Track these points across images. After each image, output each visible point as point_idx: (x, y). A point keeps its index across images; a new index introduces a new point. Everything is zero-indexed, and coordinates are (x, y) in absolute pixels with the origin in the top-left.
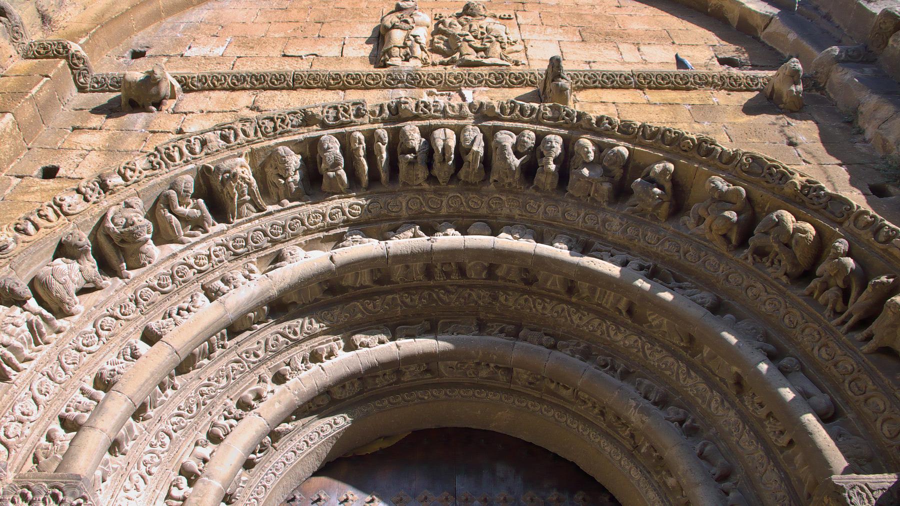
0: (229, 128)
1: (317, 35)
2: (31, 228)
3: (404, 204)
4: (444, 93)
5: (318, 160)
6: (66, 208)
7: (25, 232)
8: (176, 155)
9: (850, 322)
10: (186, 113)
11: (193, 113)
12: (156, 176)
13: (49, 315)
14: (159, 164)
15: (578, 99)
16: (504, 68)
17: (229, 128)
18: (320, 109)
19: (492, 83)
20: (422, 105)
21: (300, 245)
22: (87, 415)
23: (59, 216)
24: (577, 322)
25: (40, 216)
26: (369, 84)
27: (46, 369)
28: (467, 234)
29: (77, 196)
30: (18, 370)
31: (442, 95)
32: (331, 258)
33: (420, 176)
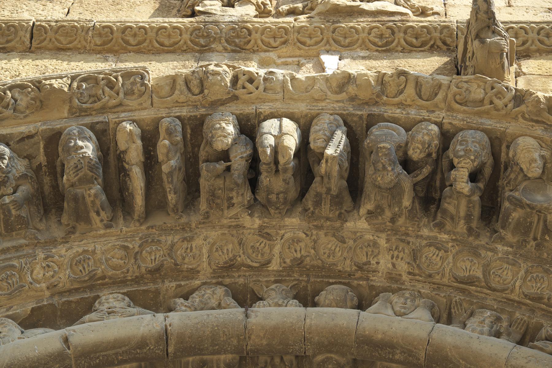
3: (205, 251)
4: (290, 60)
5: (59, 169)
15: (524, 70)
19: (375, 44)
21: (13, 318)
26: (162, 44)
28: (315, 305)
32: (66, 340)
33: (235, 201)
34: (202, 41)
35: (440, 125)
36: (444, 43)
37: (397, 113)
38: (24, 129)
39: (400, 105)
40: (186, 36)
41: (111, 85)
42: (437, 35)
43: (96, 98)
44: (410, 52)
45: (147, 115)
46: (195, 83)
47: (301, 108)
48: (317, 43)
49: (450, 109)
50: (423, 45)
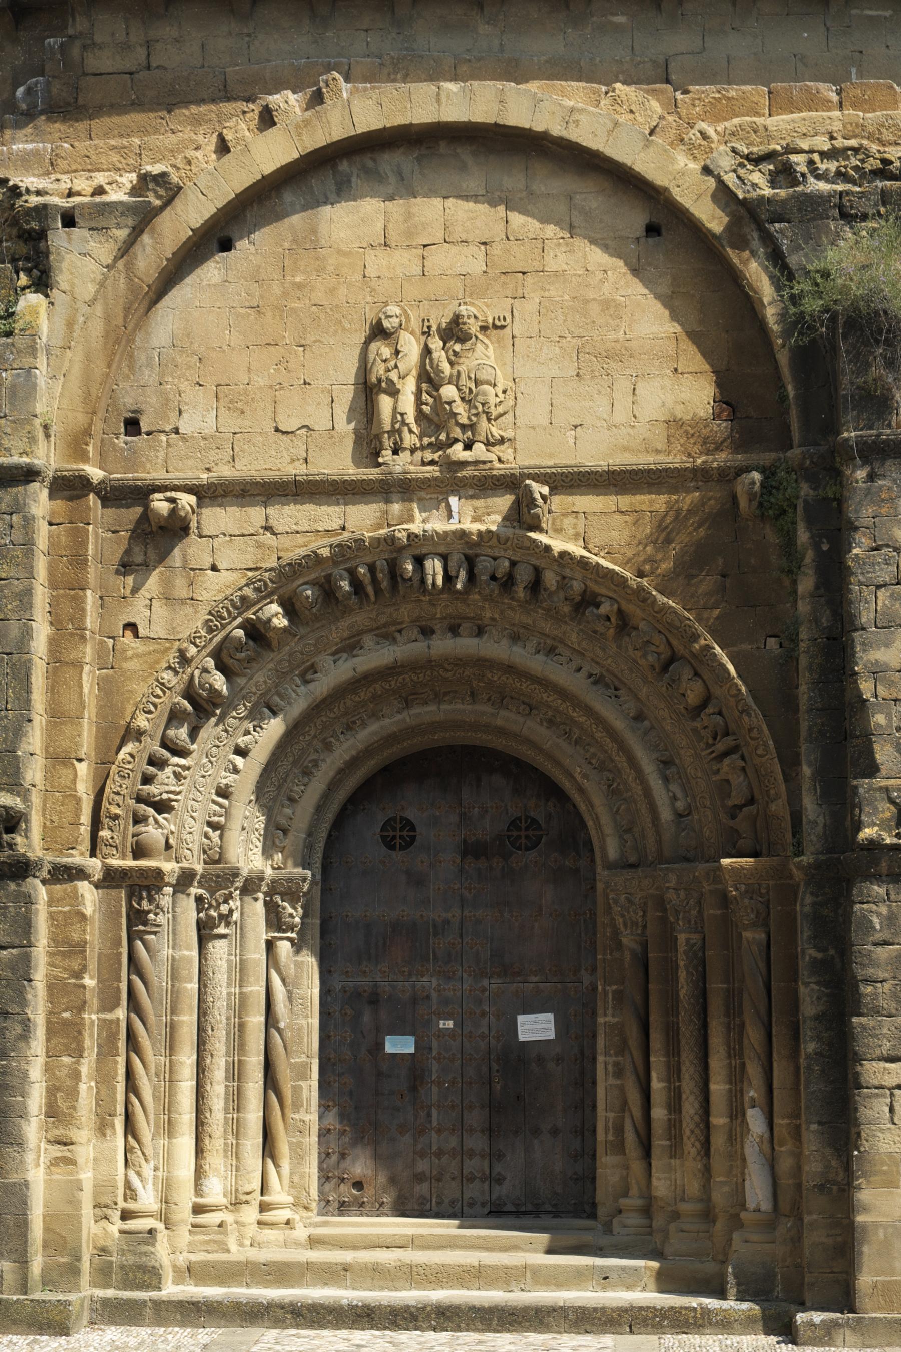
0: (260, 581)
1: (302, 381)
2: (152, 708)
4: (433, 496)
6: (167, 685)
7: (150, 712)
8: (226, 614)
9: (714, 755)
10: (210, 537)
11: (217, 536)
12: (216, 635)
13: (182, 761)
14: (215, 626)
16: (488, 466)
17: (260, 581)
18: (328, 549)
20: (412, 536)
22: (222, 819)
23: (164, 693)
24: (545, 698)
25: (155, 696)
27: (191, 796)
29: (170, 672)
30: (176, 801)
31: (431, 498)
34: (386, 487)
35: (509, 559)
36: (512, 483)
37: (489, 552)
38: (313, 576)
39: (490, 547)
40: (377, 485)
41: (350, 548)
42: (508, 479)
43: (344, 556)
44: (495, 489)
45: (369, 559)
46: (389, 541)
47: (442, 549)
48: (446, 486)
49: (514, 550)
50: (501, 485)
